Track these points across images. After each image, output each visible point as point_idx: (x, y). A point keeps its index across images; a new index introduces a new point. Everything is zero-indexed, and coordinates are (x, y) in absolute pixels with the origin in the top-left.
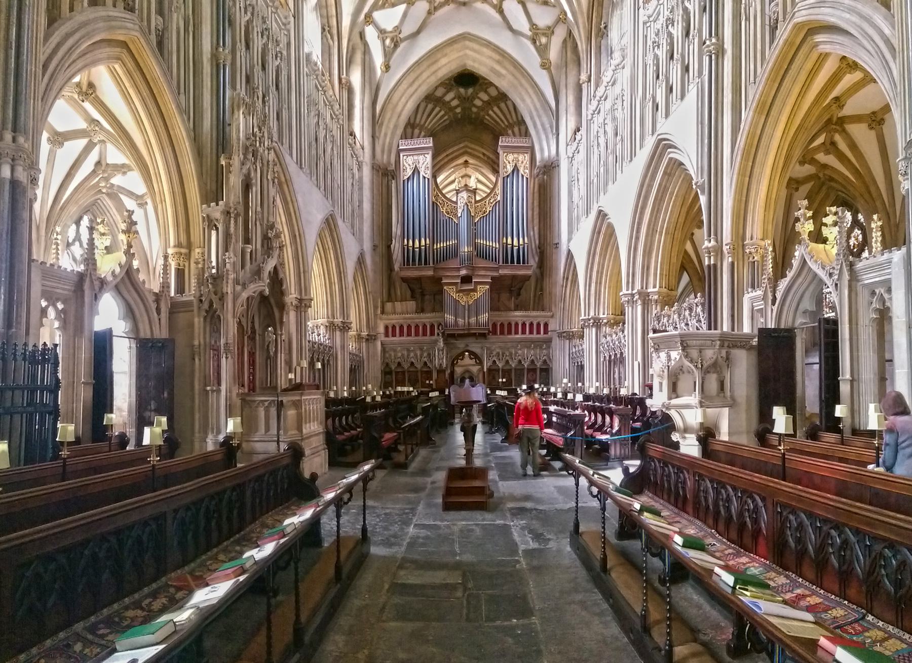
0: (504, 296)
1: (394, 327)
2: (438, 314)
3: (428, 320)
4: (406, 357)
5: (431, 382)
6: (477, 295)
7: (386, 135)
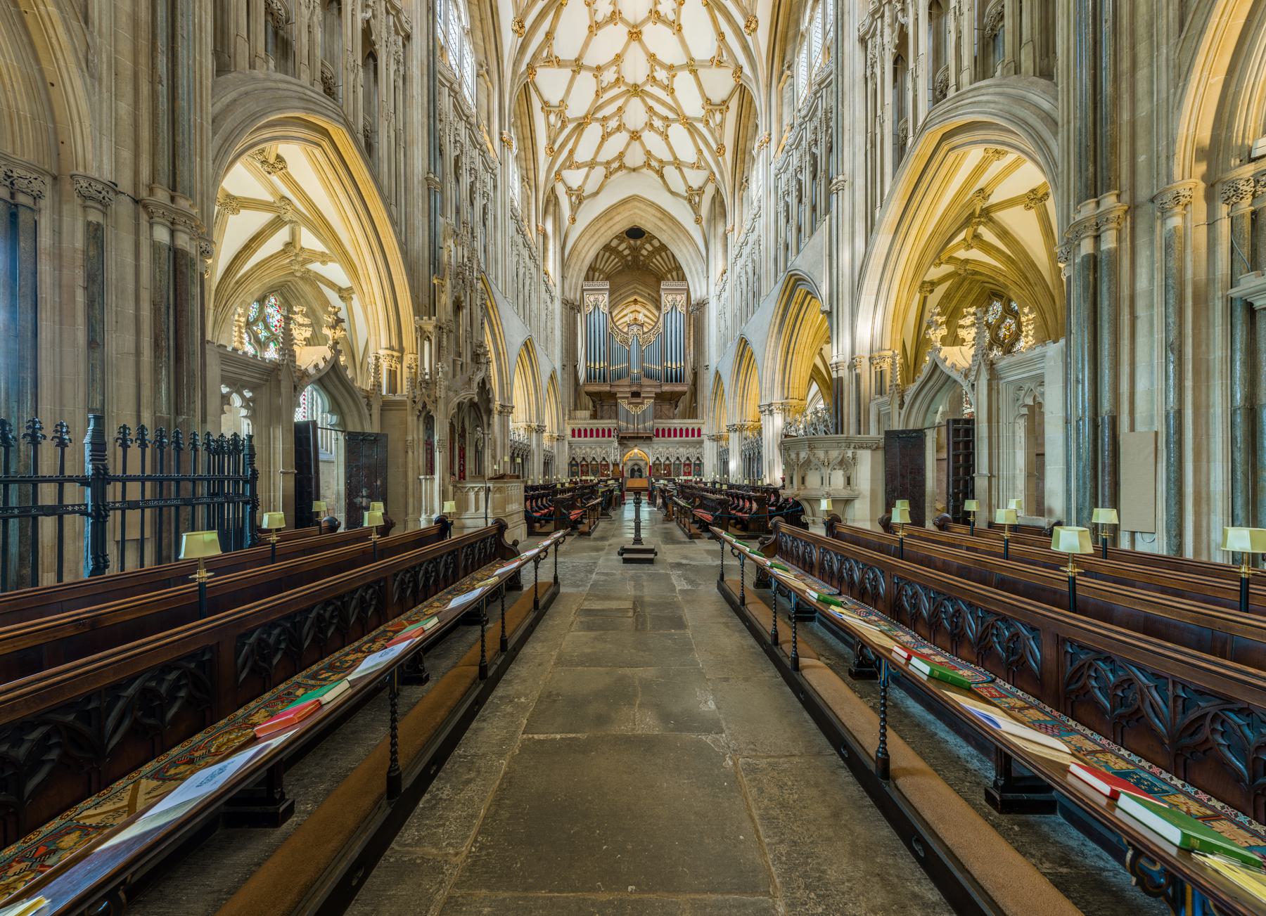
1: (580, 431)
2: (615, 421)
6: (645, 407)
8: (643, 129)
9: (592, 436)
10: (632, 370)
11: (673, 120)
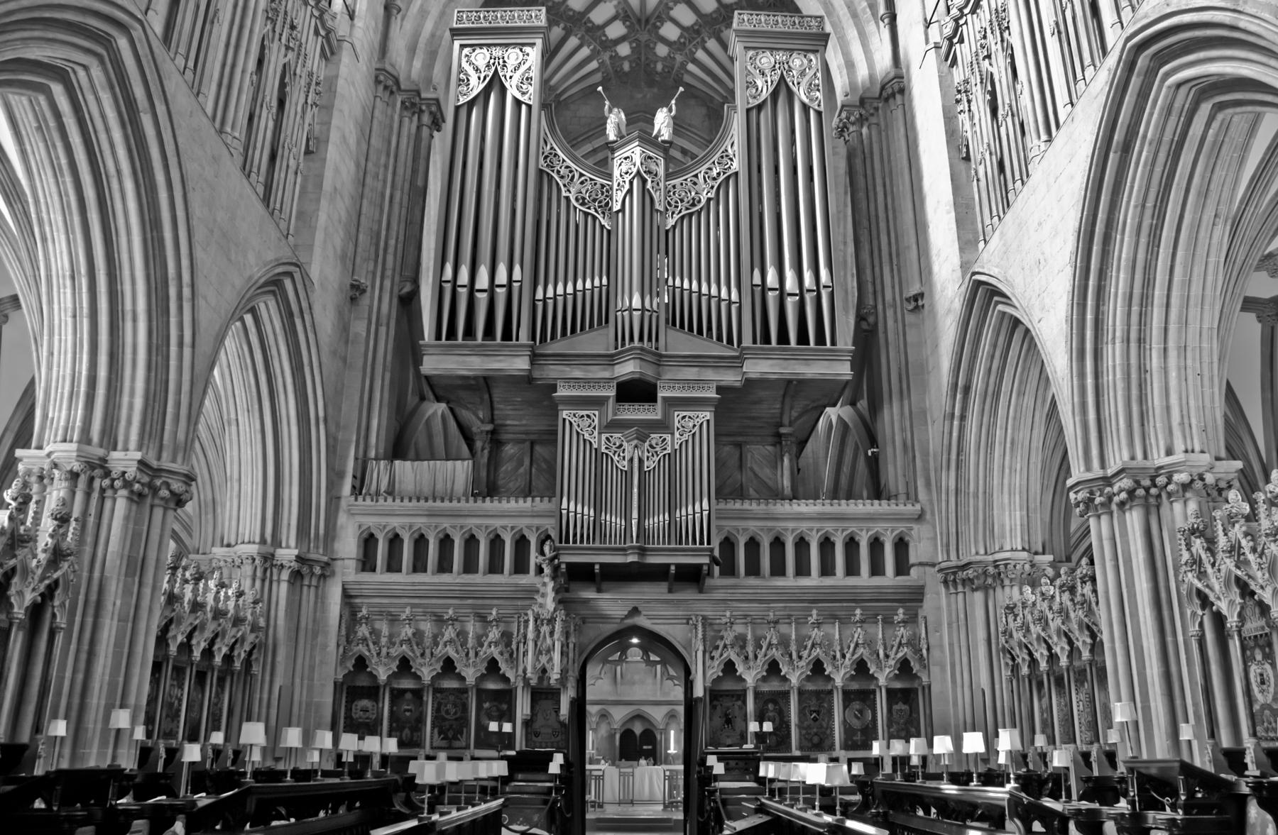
0: (758, 453)
2: (542, 505)
3: (508, 522)
4: (428, 641)
5: (507, 728)
6: (674, 440)
9: (444, 565)
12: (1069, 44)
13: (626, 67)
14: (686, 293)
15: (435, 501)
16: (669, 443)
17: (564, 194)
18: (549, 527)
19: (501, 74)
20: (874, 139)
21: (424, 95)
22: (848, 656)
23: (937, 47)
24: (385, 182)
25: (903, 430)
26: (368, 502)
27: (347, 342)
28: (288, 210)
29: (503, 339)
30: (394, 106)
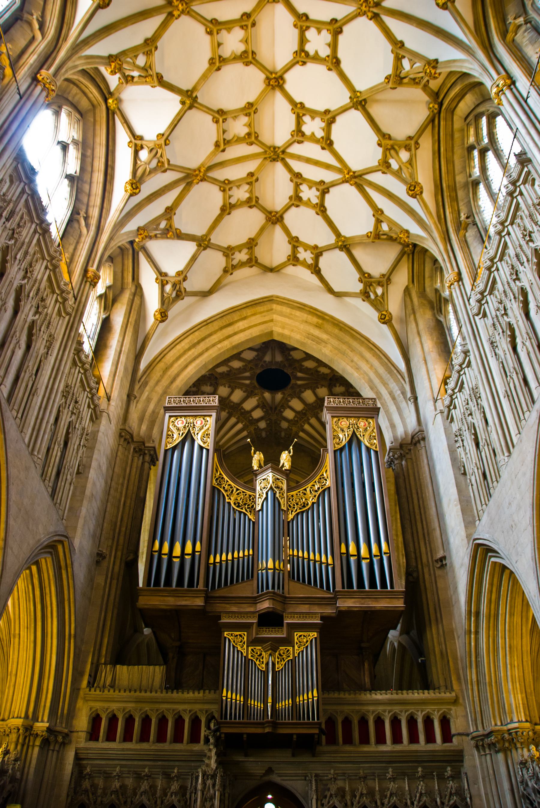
1: (113, 720)
2: (209, 695)
7: (149, 400)
8: (287, 208)
9: (144, 737)
10: (262, 564)
11: (334, 184)
12: (514, 402)
13: (264, 434)
14: (300, 559)
15: (141, 692)
16: (292, 652)
17: (227, 500)
18: (213, 710)
19: (192, 432)
20: (410, 467)
21: (146, 445)
22: (415, 803)
23: (442, 412)
24: (121, 493)
25: (439, 644)
26: (98, 692)
27: (92, 589)
28: (64, 505)
29: (189, 586)
30: (129, 450)
